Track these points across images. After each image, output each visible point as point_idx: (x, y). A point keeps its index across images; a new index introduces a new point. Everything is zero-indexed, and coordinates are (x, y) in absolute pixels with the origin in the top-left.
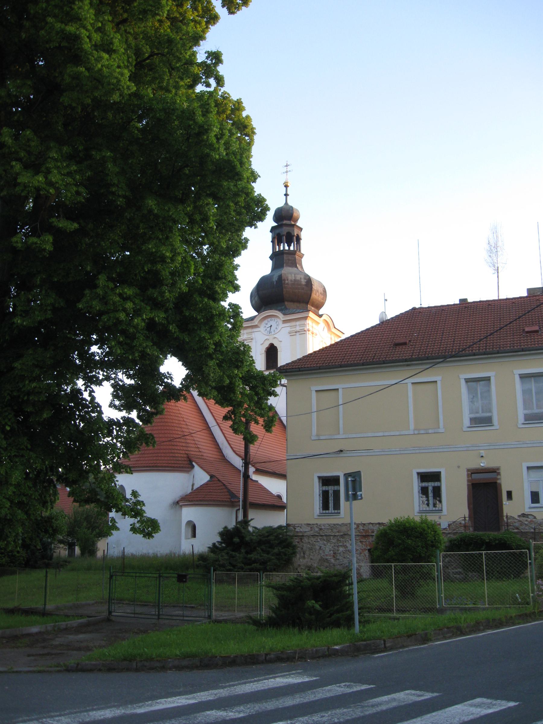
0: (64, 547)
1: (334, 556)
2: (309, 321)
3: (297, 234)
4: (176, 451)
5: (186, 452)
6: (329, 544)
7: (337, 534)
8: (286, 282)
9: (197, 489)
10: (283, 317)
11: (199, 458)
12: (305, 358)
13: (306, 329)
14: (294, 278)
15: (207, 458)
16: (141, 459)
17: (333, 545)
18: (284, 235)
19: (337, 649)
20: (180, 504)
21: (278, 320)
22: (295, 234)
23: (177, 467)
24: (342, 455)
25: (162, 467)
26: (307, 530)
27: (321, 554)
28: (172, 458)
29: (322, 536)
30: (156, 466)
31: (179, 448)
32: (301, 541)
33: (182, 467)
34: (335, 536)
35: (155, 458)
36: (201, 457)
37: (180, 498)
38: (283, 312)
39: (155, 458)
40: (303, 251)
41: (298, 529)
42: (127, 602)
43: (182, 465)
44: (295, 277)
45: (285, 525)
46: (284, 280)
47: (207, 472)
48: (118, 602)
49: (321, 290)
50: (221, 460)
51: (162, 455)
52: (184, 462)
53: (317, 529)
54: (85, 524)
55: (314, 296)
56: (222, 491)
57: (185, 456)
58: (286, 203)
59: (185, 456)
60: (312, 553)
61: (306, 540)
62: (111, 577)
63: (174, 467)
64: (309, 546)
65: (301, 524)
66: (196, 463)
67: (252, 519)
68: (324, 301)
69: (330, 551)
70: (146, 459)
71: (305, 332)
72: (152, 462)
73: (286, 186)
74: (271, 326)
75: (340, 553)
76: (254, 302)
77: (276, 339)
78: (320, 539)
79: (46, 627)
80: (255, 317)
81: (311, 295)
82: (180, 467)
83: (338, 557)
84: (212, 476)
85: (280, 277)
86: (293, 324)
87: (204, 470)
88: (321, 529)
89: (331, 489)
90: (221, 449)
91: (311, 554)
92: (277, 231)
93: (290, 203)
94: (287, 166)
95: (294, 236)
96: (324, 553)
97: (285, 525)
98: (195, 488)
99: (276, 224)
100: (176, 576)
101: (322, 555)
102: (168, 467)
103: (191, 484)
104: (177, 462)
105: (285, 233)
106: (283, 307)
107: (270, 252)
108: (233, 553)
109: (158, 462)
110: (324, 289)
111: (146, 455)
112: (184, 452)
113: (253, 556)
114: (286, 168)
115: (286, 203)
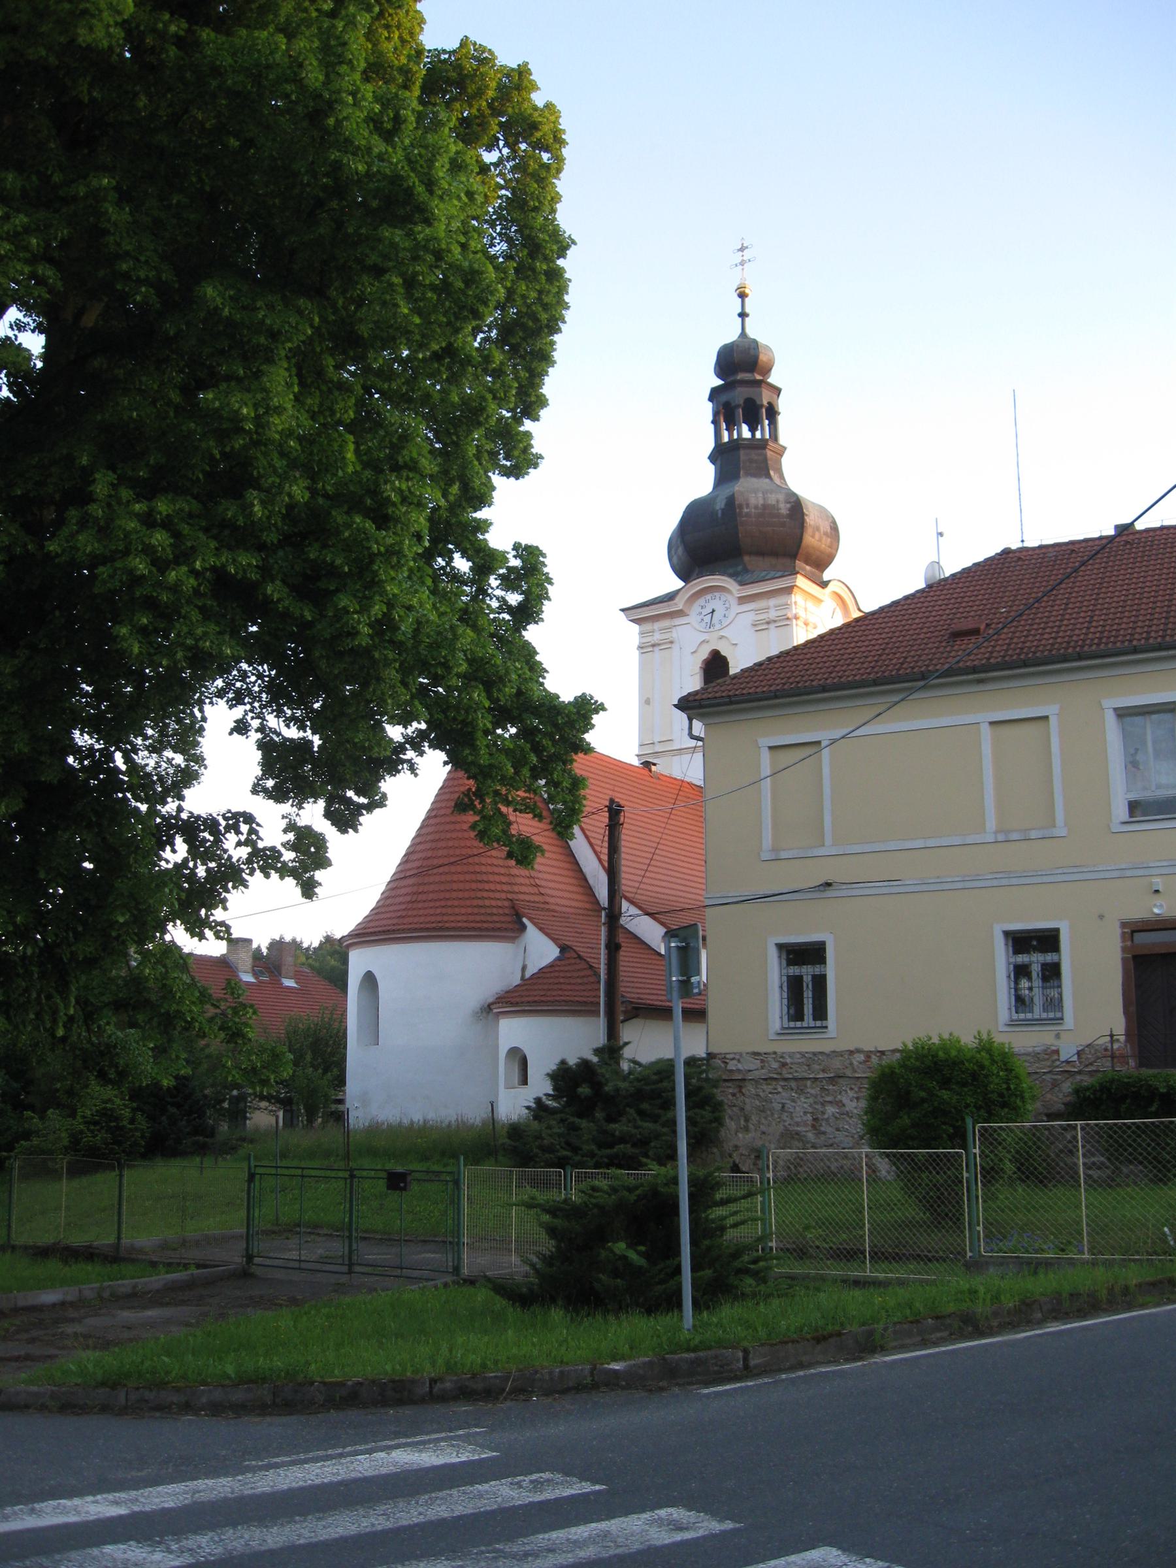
0: (270, 1108)
1: (813, 1126)
2: (797, 597)
3: (769, 403)
4: (485, 894)
5: (510, 896)
6: (803, 1100)
7: (821, 1076)
8: (745, 510)
10: (739, 590)
11: (538, 909)
12: (746, 674)
13: (790, 615)
14: (761, 502)
15: (557, 908)
16: (410, 913)
17: (811, 1100)
18: (738, 406)
19: (615, 1371)
20: (495, 1011)
21: (729, 597)
22: (765, 403)
23: (487, 929)
24: (830, 893)
25: (454, 929)
26: (752, 1067)
27: (785, 1121)
28: (476, 910)
29: (786, 1079)
30: (441, 929)
31: (492, 887)
32: (740, 1092)
33: (499, 929)
34: (816, 1079)
35: (438, 911)
36: (542, 906)
38: (739, 579)
39: (438, 911)
40: (782, 440)
41: (732, 1065)
42: (325, 1231)
43: (498, 925)
44: (764, 499)
45: (704, 1055)
46: (741, 506)
47: (554, 940)
48: (309, 1230)
49: (825, 526)
50: (590, 913)
51: (456, 903)
52: (502, 919)
53: (775, 1065)
54: (309, 1057)
55: (811, 539)
56: (585, 980)
57: (506, 904)
58: (743, 334)
59: (506, 904)
60: (766, 1118)
61: (750, 1089)
62: (251, 1177)
63: (480, 929)
64: (757, 1103)
65: (741, 1054)
66: (530, 919)
67: (626, 1044)
68: (834, 551)
69: (805, 1113)
70: (421, 912)
72: (433, 919)
73: (742, 296)
74: (713, 611)
75: (827, 1120)
76: (675, 559)
77: (723, 639)
78: (783, 1087)
79: (80, 1291)
80: (677, 592)
81: (800, 538)
82: (493, 929)
83: (823, 1129)
84: (564, 949)
85: (731, 501)
86: (762, 604)
87: (547, 935)
88: (784, 1065)
89: (807, 972)
90: (590, 888)
91: (763, 1121)
92: (724, 398)
93: (752, 333)
94: (742, 249)
95: (762, 406)
96: (792, 1118)
97: (704, 1055)
98: (528, 975)
99: (722, 382)
100: (384, 1175)
101: (786, 1124)
102: (469, 929)
104: (489, 918)
105: (741, 402)
106: (740, 568)
107: (711, 445)
108: (577, 1120)
109: (445, 918)
110: (834, 522)
111: (420, 905)
112: (503, 896)
113: (617, 1128)
114: (741, 253)
115: (743, 334)
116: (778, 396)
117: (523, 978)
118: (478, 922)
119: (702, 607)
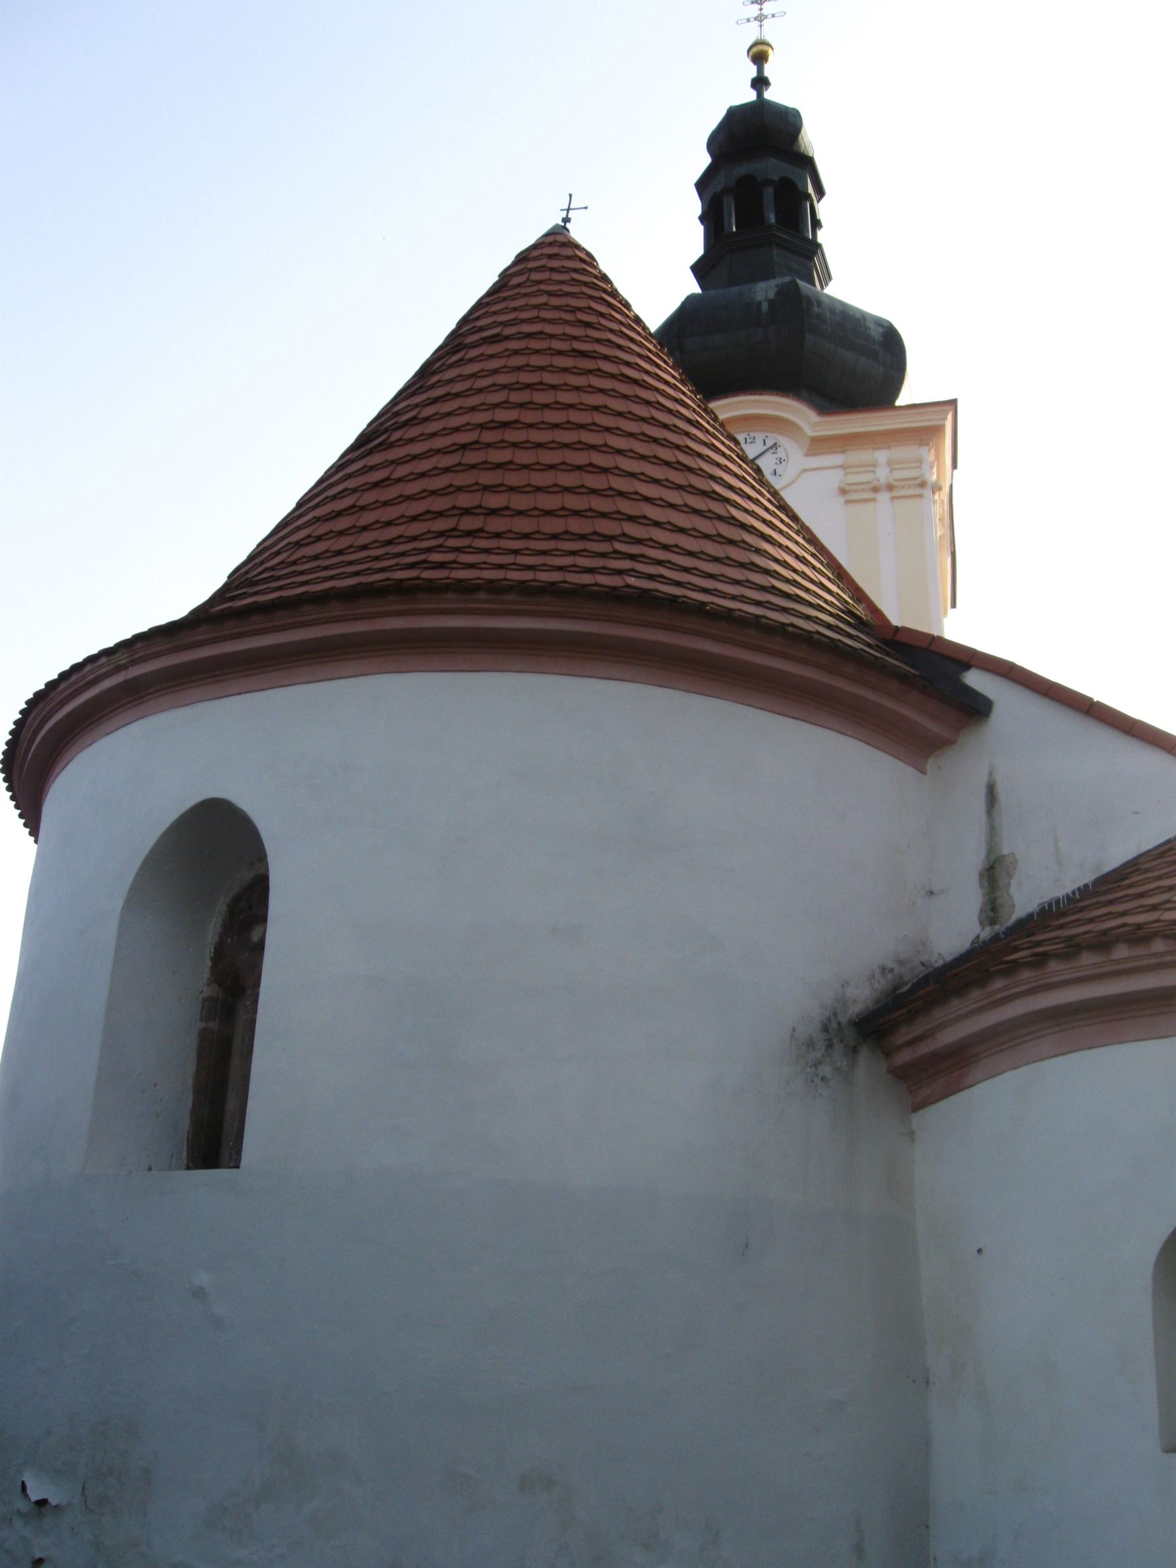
8: (816, 310)
18: (768, 182)
21: (783, 440)
37: (882, 984)
71: (918, 491)
73: (759, 57)
103: (974, 857)
105: (776, 178)
116: (818, 202)
117: (992, 909)
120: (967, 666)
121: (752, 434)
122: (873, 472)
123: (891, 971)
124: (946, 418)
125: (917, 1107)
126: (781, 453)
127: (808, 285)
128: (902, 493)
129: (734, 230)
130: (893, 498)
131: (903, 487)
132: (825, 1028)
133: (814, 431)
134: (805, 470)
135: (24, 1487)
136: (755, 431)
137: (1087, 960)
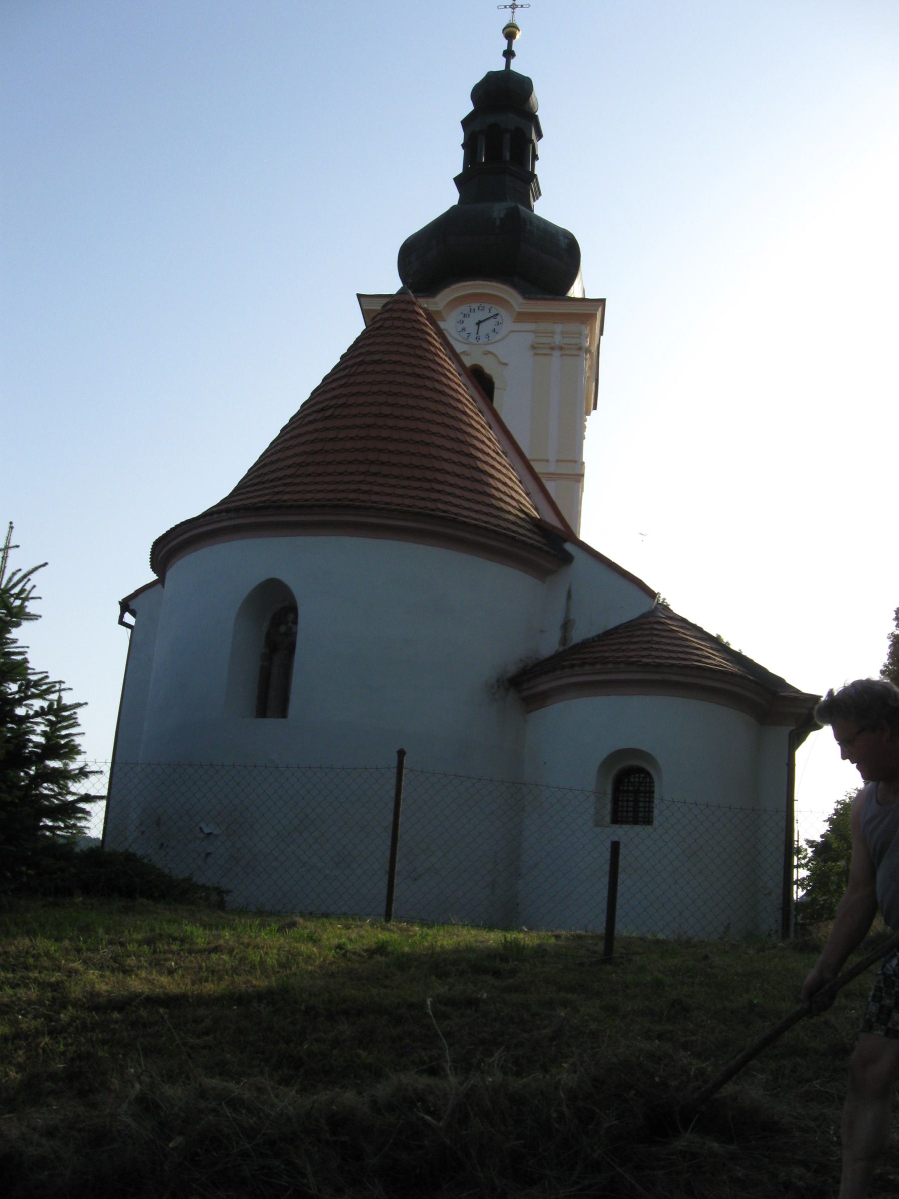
9: (585, 645)
21: (502, 312)
86: (542, 326)
98: (578, 635)
112: (514, 503)
116: (538, 141)
117: (564, 639)
118: (504, 529)
119: (465, 316)
120: (565, 541)
121: (483, 305)
122: (552, 337)
123: (524, 661)
124: (598, 310)
125: (529, 712)
126: (499, 319)
127: (525, 209)
128: (568, 352)
129: (483, 161)
130: (562, 355)
131: (568, 349)
132: (498, 681)
133: (520, 308)
134: (512, 331)
135: (201, 829)
136: (484, 302)
137: (587, 668)
